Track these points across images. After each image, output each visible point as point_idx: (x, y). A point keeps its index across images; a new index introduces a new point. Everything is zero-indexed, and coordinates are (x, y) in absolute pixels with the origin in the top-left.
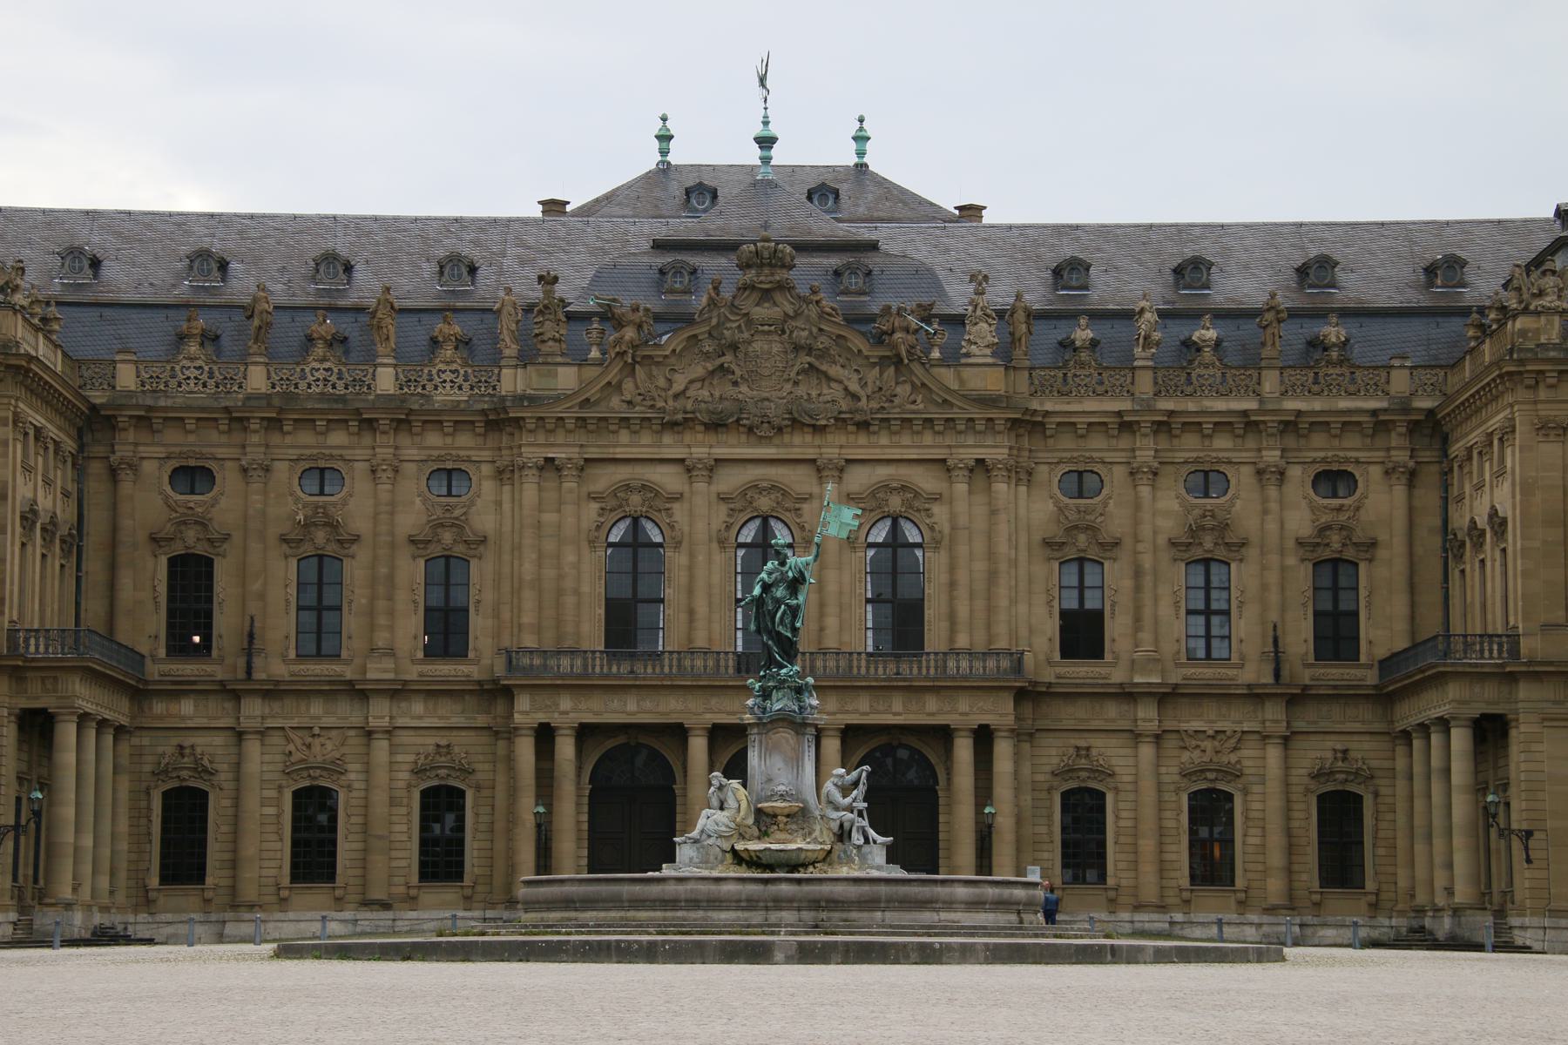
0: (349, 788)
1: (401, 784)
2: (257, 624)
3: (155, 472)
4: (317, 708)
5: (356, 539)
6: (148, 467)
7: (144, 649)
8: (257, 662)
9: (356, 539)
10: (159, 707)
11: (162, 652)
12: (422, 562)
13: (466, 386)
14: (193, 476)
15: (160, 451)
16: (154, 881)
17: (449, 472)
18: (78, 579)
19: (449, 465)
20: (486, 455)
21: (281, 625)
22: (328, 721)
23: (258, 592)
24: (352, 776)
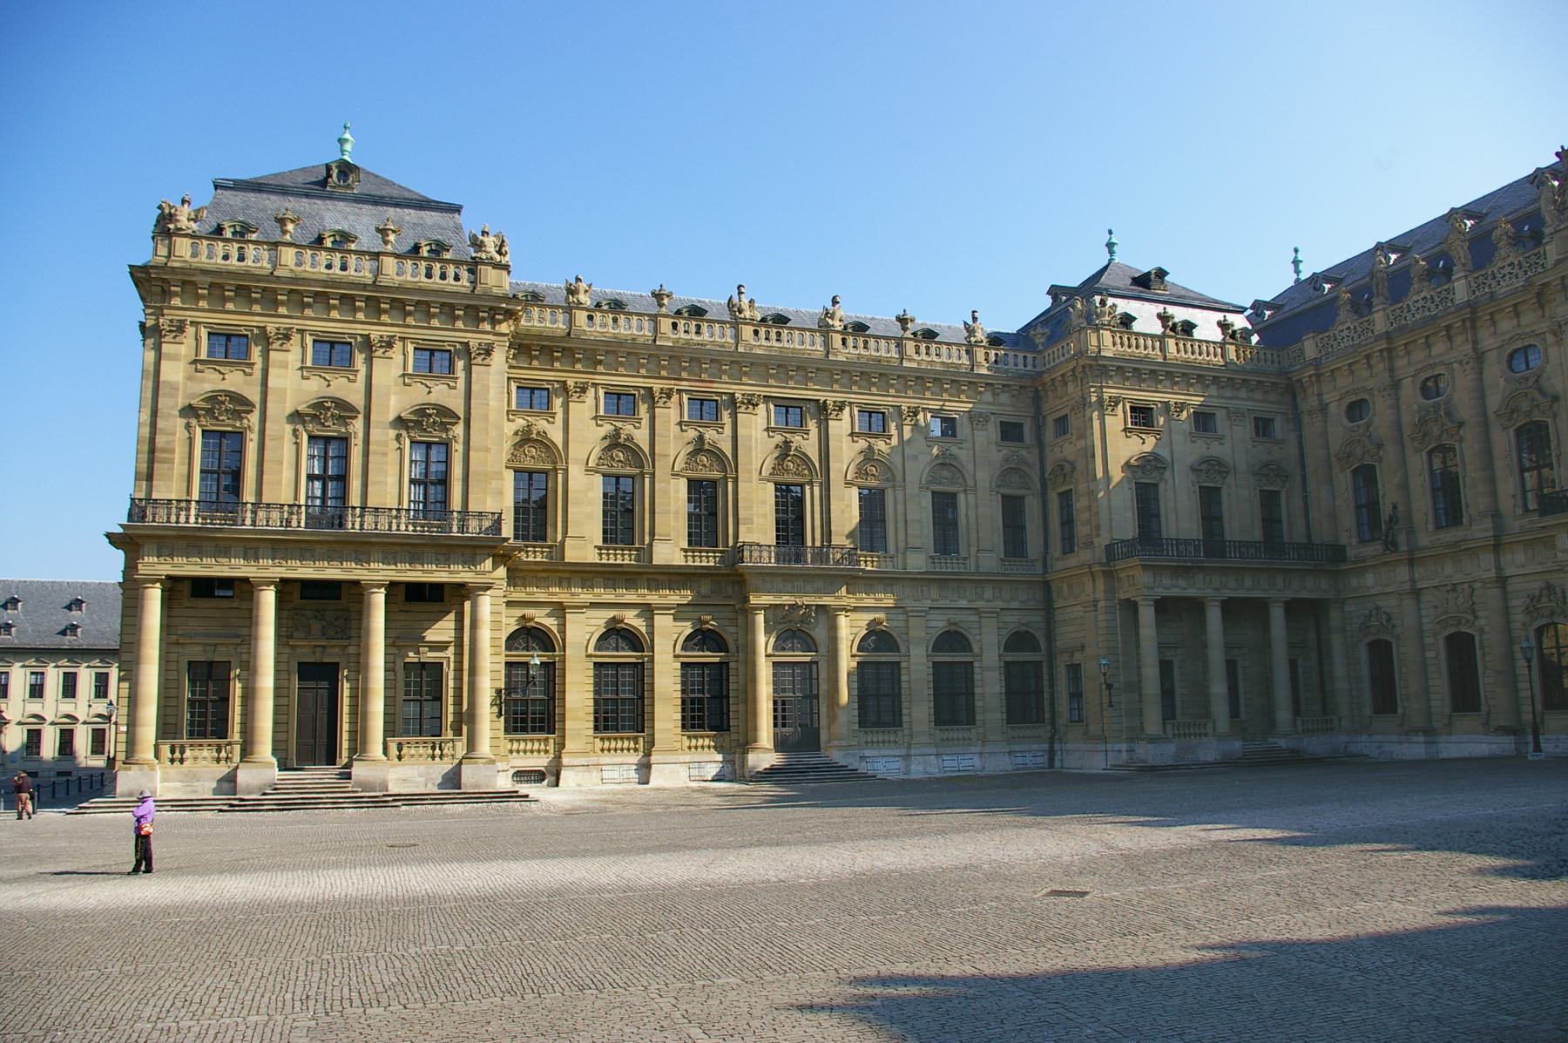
0: (1481, 630)
1: (1518, 625)
2: (1400, 508)
3: (1336, 410)
4: (1448, 569)
5: (1461, 424)
6: (1333, 408)
7: (1344, 541)
8: (1402, 539)
9: (1461, 424)
10: (1354, 582)
11: (1354, 541)
12: (1511, 432)
13: (1521, 273)
14: (1356, 409)
15: (1335, 394)
16: (1368, 712)
17: (1525, 349)
18: (1305, 498)
19: (1519, 344)
20: (1545, 326)
21: (1422, 504)
22: (1457, 578)
23: (1407, 483)
24: (1482, 622)
